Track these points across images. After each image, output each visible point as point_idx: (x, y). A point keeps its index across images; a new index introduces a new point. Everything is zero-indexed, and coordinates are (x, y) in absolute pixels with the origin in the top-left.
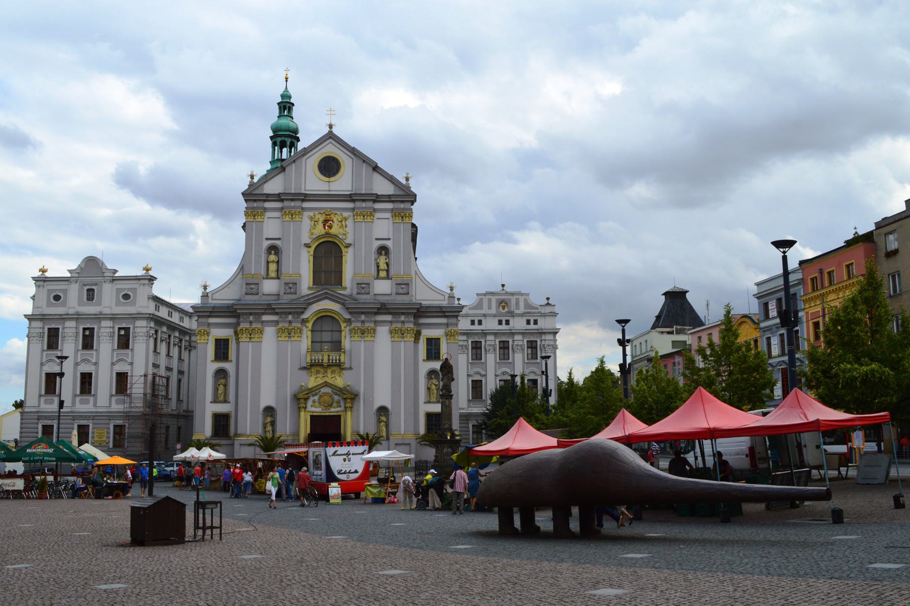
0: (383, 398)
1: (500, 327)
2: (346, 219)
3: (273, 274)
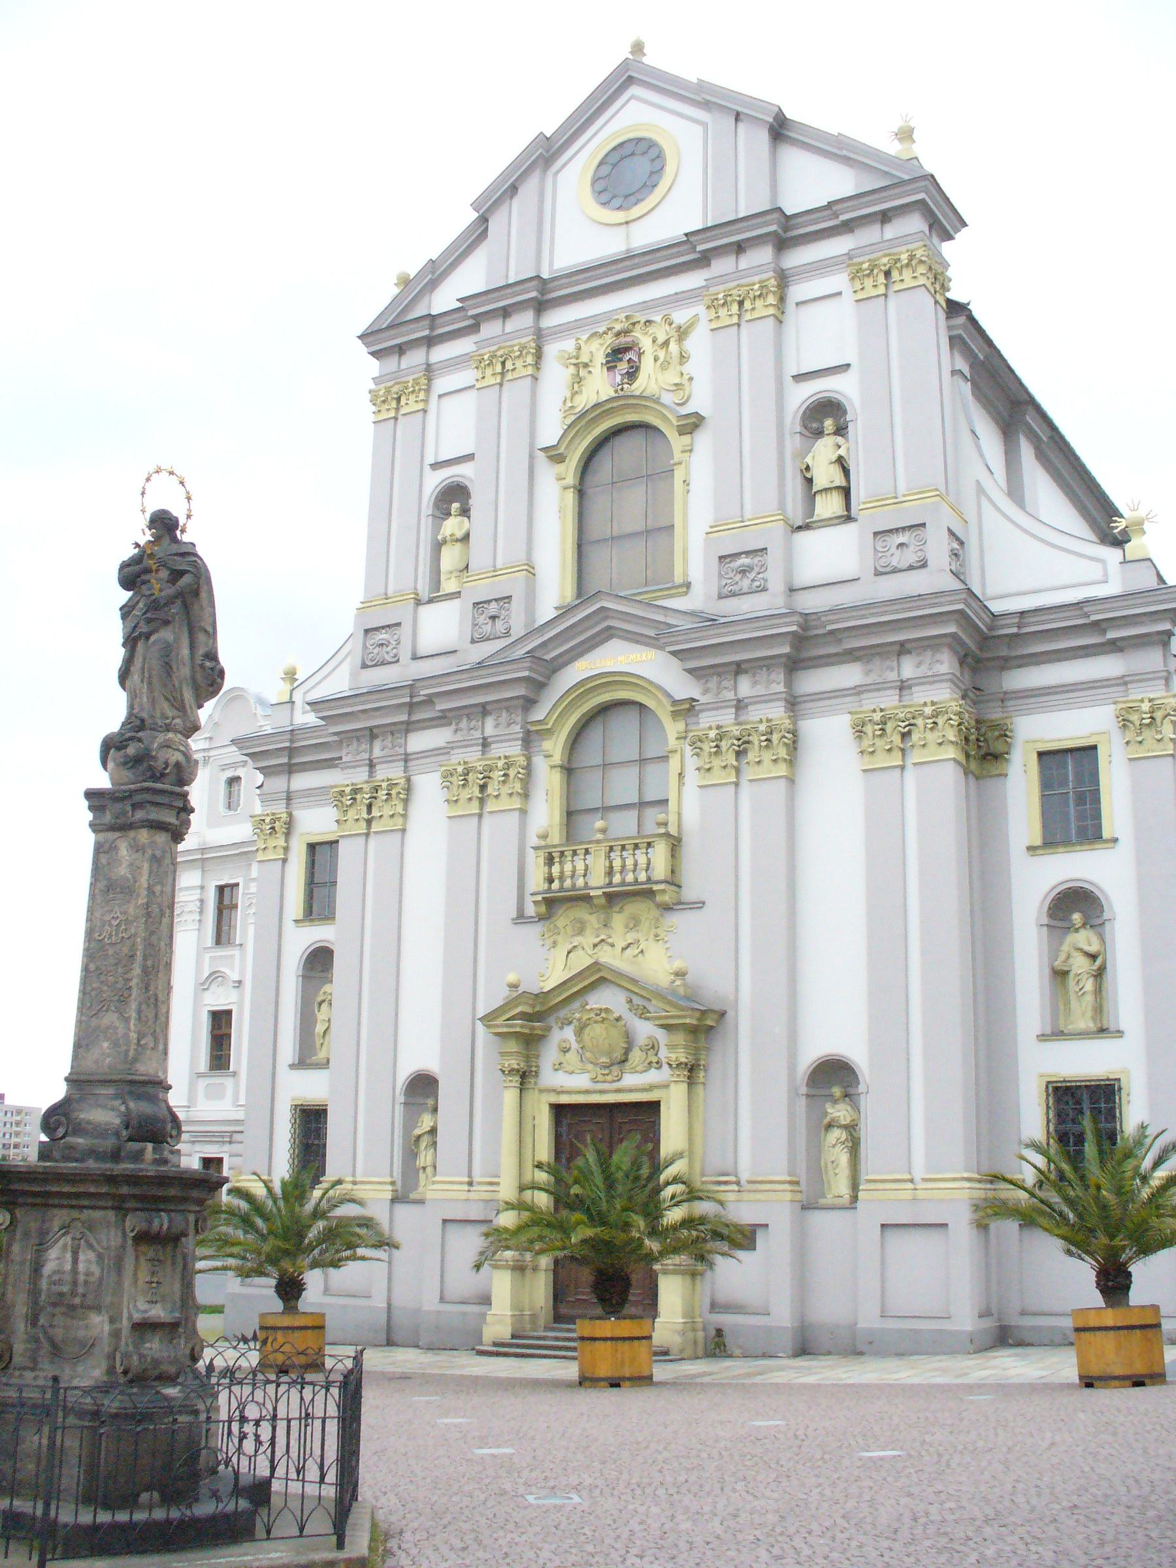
0: (836, 1025)
2: (682, 333)
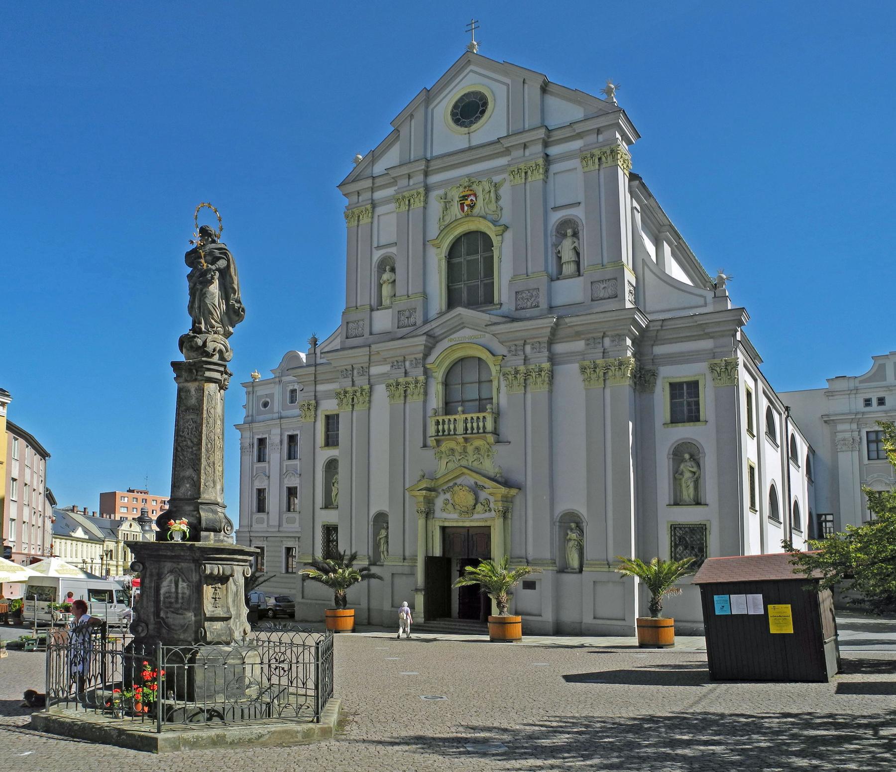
0: (573, 501)
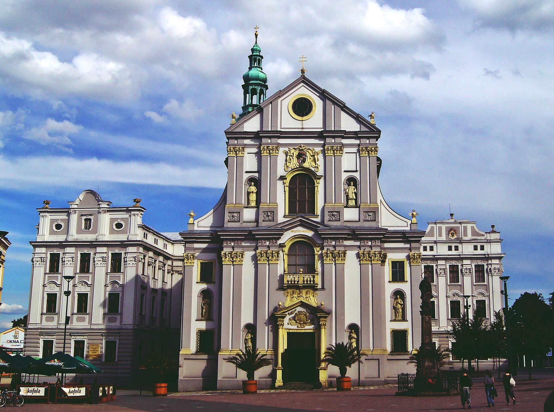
1: (450, 253)
3: (253, 204)
